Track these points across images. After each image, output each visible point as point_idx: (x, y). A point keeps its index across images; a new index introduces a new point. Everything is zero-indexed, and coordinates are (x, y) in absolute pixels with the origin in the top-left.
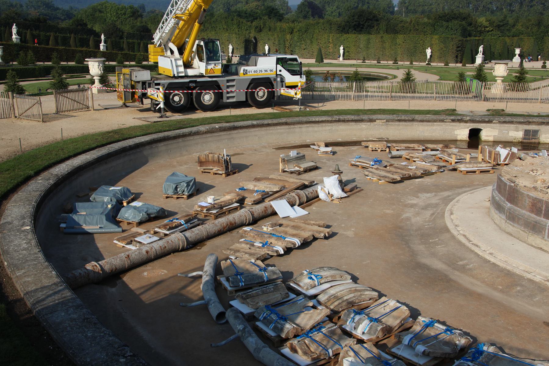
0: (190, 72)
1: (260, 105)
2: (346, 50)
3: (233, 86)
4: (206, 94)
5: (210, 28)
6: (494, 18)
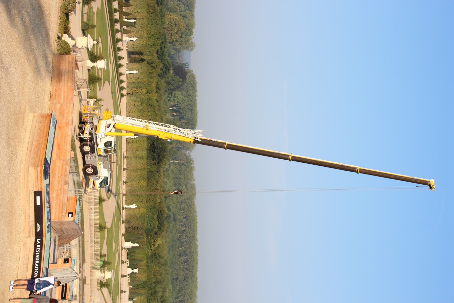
5: (151, 18)
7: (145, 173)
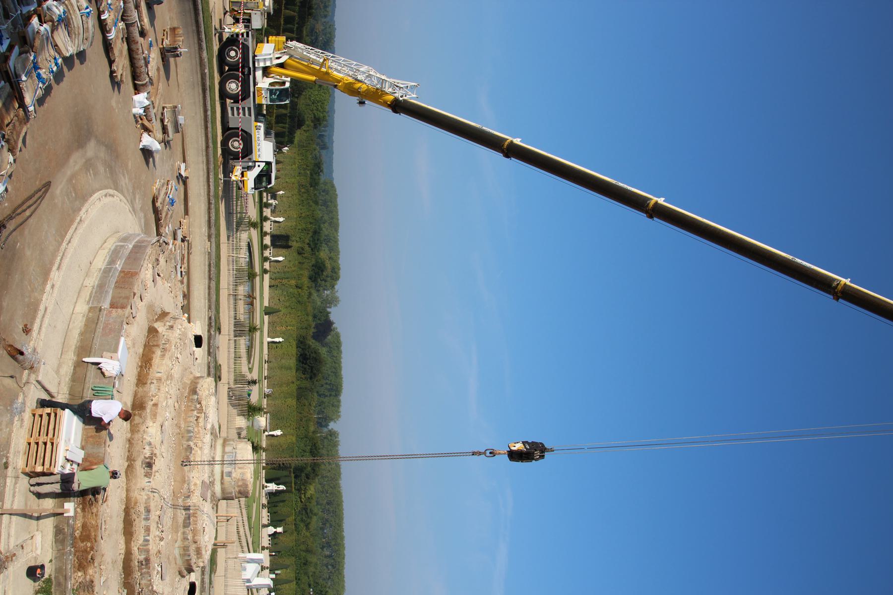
0: (259, 74)
1: (225, 143)
2: (279, 345)
3: (244, 115)
4: (237, 85)
6: (314, 502)
7: (294, 387)
